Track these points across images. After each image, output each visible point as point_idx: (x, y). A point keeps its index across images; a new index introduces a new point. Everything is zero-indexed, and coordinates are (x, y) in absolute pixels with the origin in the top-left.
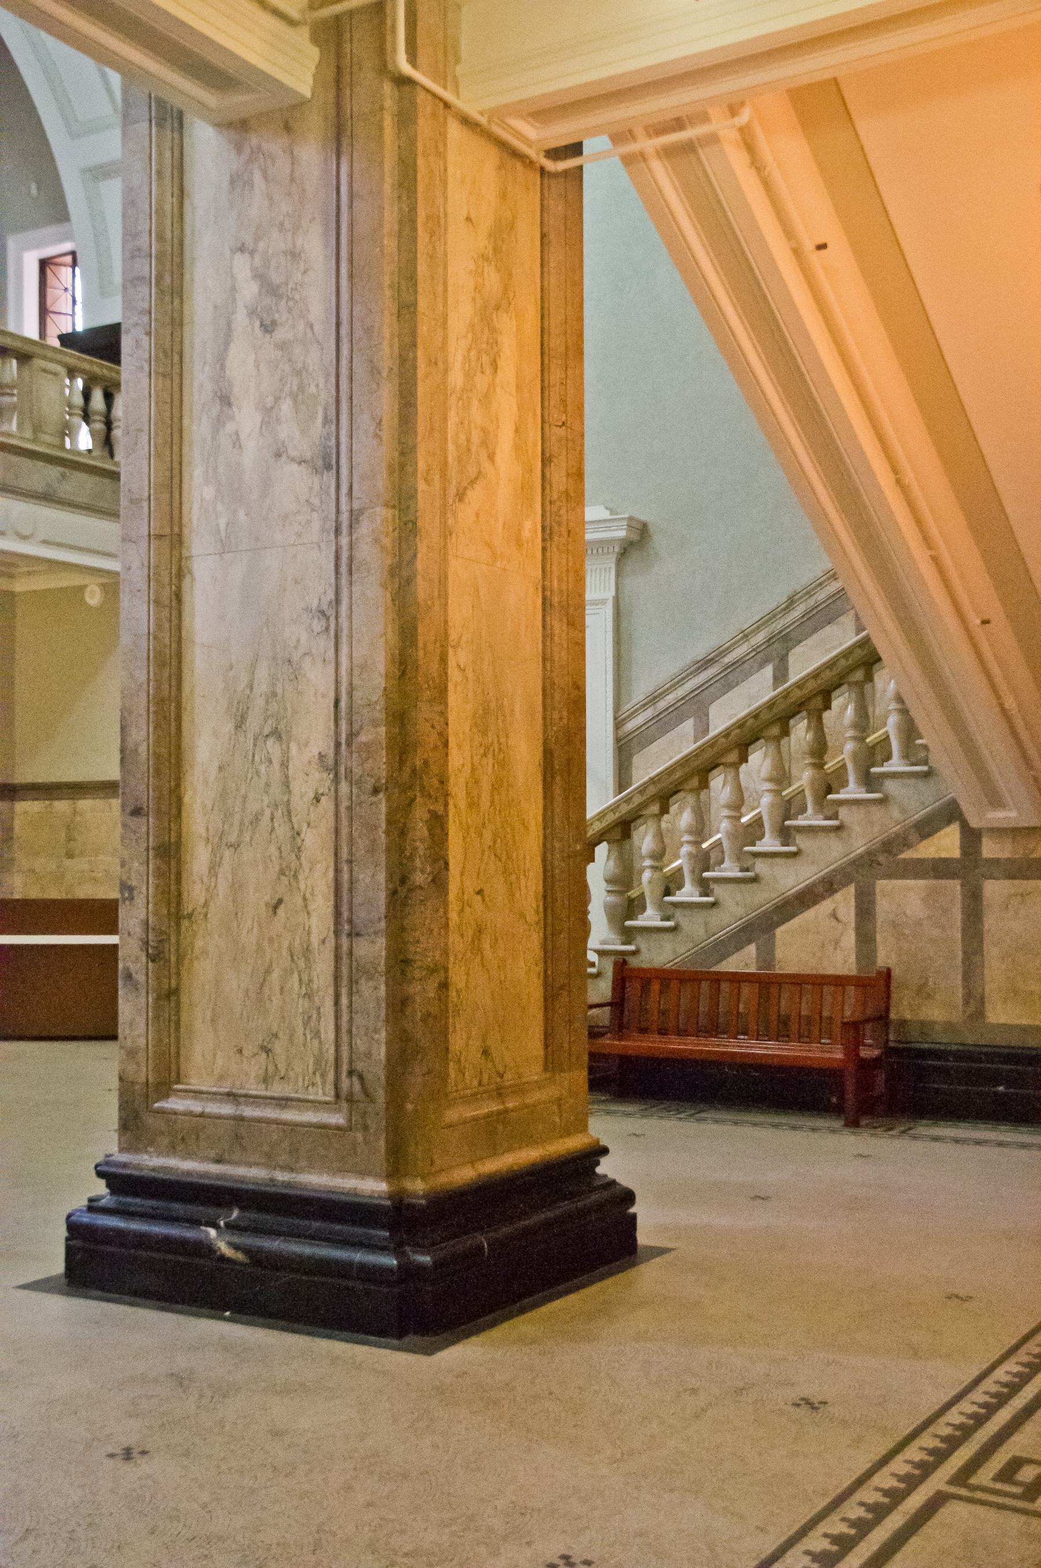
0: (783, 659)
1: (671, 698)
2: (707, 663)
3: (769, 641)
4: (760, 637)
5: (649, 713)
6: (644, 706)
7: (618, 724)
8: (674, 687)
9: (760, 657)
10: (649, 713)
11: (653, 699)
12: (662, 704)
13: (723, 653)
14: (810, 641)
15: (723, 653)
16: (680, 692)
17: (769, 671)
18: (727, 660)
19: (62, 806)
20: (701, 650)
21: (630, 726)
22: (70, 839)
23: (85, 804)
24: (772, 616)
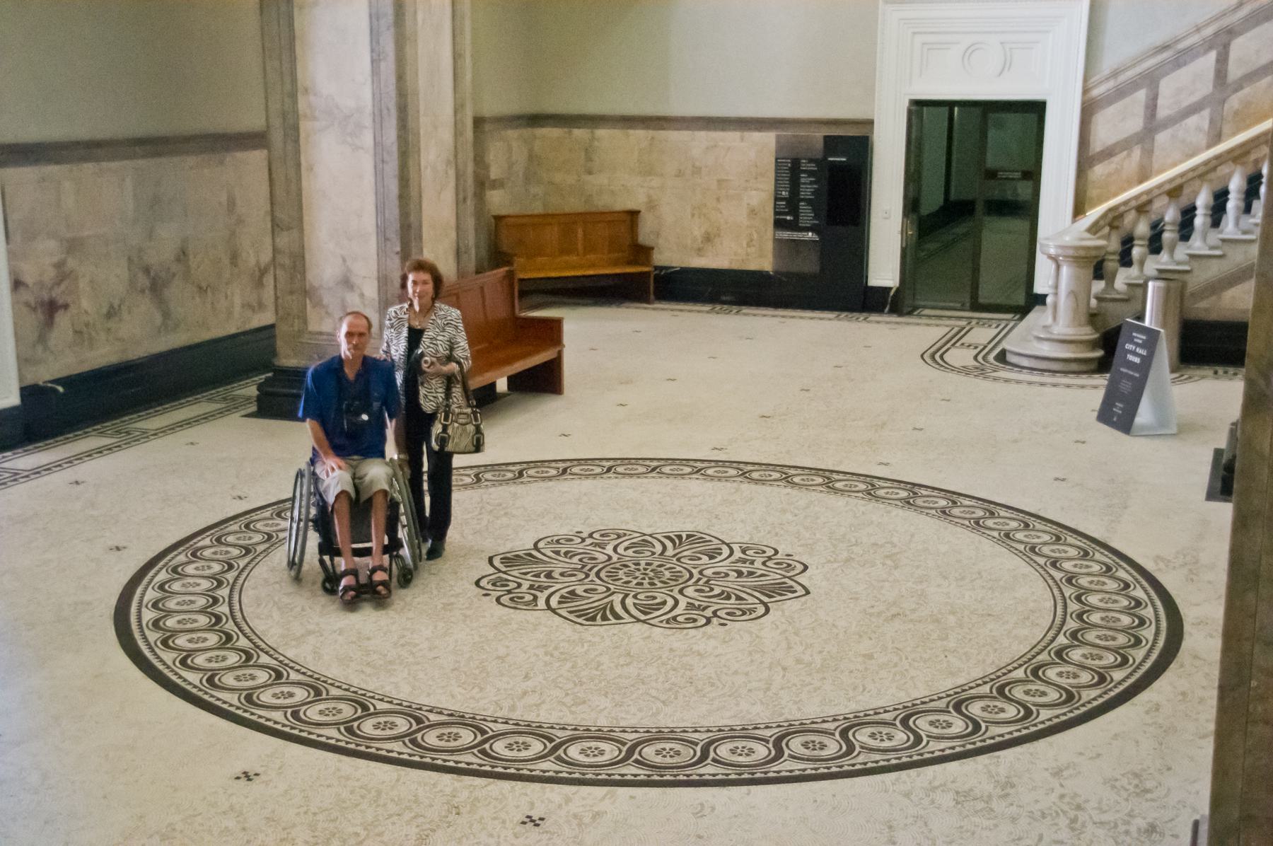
0: (1226, 47)
1: (1130, 74)
2: (1165, 47)
3: (1216, 34)
4: (1209, 31)
5: (1111, 84)
6: (1107, 79)
7: (1085, 91)
8: (1134, 65)
9: (1208, 45)
10: (1111, 84)
11: (1115, 74)
12: (1122, 78)
13: (1178, 41)
14: (1249, 35)
15: (1178, 41)
16: (1138, 69)
17: (1213, 55)
18: (1181, 46)
19: (580, 133)
20: (1159, 38)
21: (1095, 93)
22: (589, 159)
23: (602, 132)
24: (1223, 14)
